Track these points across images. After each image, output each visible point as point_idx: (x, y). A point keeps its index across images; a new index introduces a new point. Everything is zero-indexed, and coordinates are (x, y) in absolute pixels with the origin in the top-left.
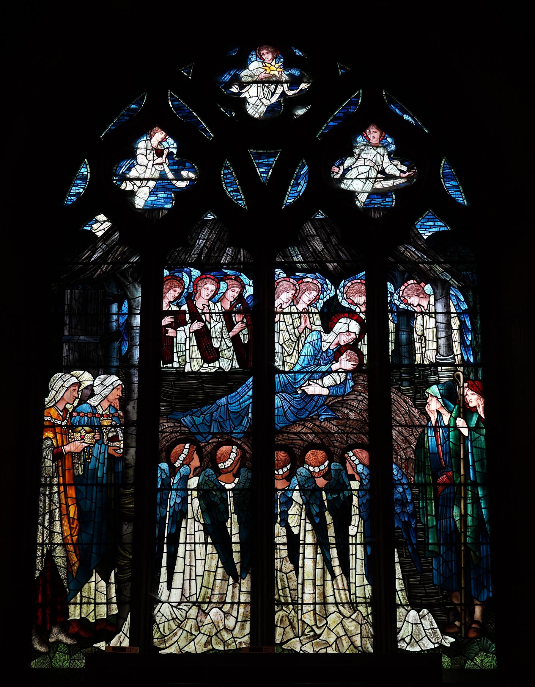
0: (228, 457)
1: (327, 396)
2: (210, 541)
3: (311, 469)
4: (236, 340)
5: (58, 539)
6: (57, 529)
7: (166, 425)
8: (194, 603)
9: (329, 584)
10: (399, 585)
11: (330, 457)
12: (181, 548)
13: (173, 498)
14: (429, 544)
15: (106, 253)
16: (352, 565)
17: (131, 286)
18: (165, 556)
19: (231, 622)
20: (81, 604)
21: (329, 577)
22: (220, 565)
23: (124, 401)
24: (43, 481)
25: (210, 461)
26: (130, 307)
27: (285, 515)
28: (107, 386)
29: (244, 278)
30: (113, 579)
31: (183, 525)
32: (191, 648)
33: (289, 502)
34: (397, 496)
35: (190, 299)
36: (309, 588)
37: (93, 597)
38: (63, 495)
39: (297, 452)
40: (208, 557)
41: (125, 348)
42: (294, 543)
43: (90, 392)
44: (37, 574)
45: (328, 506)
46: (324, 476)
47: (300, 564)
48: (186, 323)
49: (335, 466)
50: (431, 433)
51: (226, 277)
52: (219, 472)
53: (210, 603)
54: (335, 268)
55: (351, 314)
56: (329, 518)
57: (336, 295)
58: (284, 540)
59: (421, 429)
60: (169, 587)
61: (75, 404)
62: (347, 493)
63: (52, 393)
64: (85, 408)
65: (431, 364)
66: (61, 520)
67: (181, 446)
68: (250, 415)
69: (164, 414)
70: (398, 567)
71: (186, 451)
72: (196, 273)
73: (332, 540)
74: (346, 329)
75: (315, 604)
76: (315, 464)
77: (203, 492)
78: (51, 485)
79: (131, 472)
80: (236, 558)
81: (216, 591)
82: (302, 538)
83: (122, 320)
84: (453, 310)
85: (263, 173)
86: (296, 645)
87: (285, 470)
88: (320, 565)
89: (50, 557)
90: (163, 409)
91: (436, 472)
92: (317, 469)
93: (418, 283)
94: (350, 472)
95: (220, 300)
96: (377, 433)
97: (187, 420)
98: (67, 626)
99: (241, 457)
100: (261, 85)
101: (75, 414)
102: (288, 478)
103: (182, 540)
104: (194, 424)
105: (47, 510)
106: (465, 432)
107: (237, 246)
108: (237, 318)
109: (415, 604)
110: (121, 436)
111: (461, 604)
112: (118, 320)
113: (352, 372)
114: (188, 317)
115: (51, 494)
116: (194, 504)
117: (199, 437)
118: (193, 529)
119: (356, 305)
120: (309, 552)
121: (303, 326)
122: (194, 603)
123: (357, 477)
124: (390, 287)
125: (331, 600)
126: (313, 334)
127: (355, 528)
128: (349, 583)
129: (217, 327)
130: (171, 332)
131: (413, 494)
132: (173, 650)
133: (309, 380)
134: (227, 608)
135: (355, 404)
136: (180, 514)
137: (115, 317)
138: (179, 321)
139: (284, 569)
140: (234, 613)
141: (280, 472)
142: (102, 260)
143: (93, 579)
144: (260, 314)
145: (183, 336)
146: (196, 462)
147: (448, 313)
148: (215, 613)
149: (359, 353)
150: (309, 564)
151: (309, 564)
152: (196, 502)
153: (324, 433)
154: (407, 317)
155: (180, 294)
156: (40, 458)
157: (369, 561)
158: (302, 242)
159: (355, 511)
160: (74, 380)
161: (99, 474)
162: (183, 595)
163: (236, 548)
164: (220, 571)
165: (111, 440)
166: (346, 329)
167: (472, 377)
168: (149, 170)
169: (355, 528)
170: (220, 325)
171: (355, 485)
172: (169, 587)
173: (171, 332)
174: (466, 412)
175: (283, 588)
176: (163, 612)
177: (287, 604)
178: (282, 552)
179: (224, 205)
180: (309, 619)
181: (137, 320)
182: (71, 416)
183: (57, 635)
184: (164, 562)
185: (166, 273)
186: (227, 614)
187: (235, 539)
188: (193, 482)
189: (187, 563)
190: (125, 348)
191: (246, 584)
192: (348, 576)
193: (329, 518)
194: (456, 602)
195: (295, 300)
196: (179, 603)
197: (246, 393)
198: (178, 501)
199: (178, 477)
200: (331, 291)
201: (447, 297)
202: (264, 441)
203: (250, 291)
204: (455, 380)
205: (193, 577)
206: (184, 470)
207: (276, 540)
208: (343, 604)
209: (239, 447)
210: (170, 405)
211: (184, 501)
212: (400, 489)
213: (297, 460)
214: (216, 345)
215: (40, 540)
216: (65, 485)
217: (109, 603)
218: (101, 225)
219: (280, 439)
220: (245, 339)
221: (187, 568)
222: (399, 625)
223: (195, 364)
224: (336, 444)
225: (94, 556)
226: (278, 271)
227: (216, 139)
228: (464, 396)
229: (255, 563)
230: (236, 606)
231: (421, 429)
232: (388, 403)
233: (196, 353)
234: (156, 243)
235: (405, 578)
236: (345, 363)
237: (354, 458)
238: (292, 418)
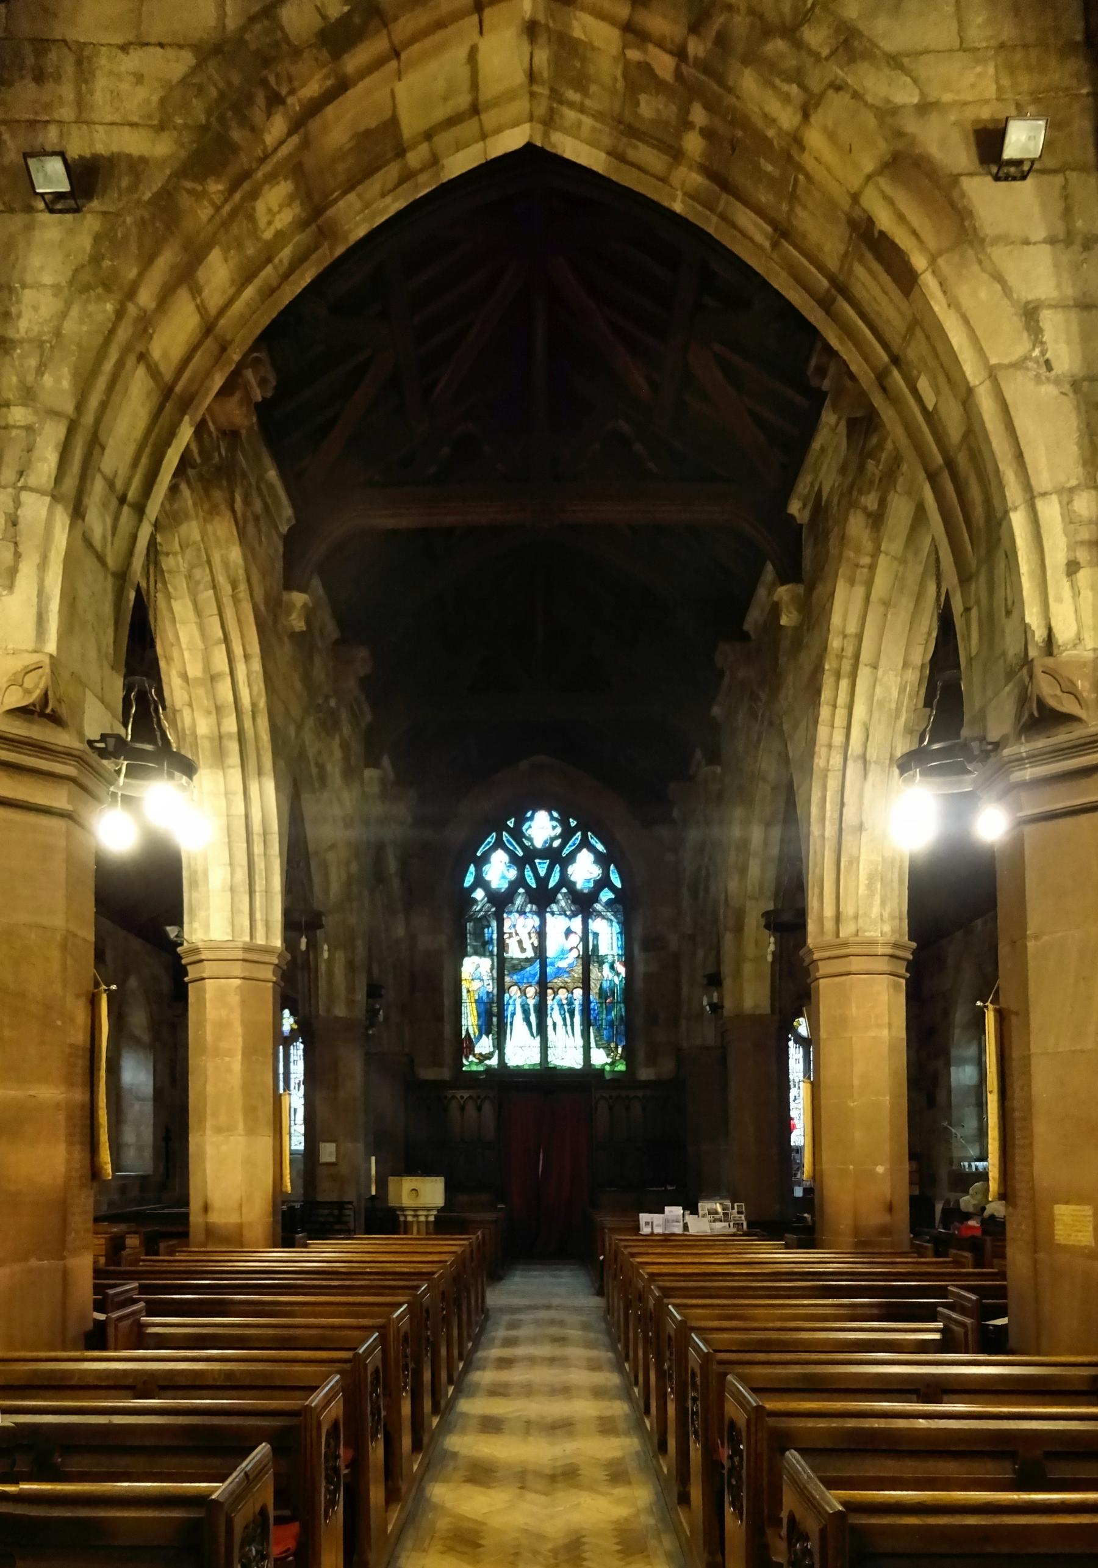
0: (531, 991)
6: (470, 1020)
7: (507, 979)
13: (511, 1008)
25: (524, 993)
35: (514, 926)
43: (478, 966)
72: (517, 915)
74: (575, 940)
77: (523, 1006)
85: (542, 872)
97: (515, 977)
98: (474, 1055)
126: (562, 934)
130: (507, 941)
136: (513, 1014)
142: (481, 910)
144: (541, 933)
146: (519, 994)
181: (495, 936)
183: (471, 1058)
191: (538, 1038)
197: (537, 965)
220: (536, 944)
225: (485, 1028)
233: (518, 949)
234: (501, 902)
236: (575, 953)
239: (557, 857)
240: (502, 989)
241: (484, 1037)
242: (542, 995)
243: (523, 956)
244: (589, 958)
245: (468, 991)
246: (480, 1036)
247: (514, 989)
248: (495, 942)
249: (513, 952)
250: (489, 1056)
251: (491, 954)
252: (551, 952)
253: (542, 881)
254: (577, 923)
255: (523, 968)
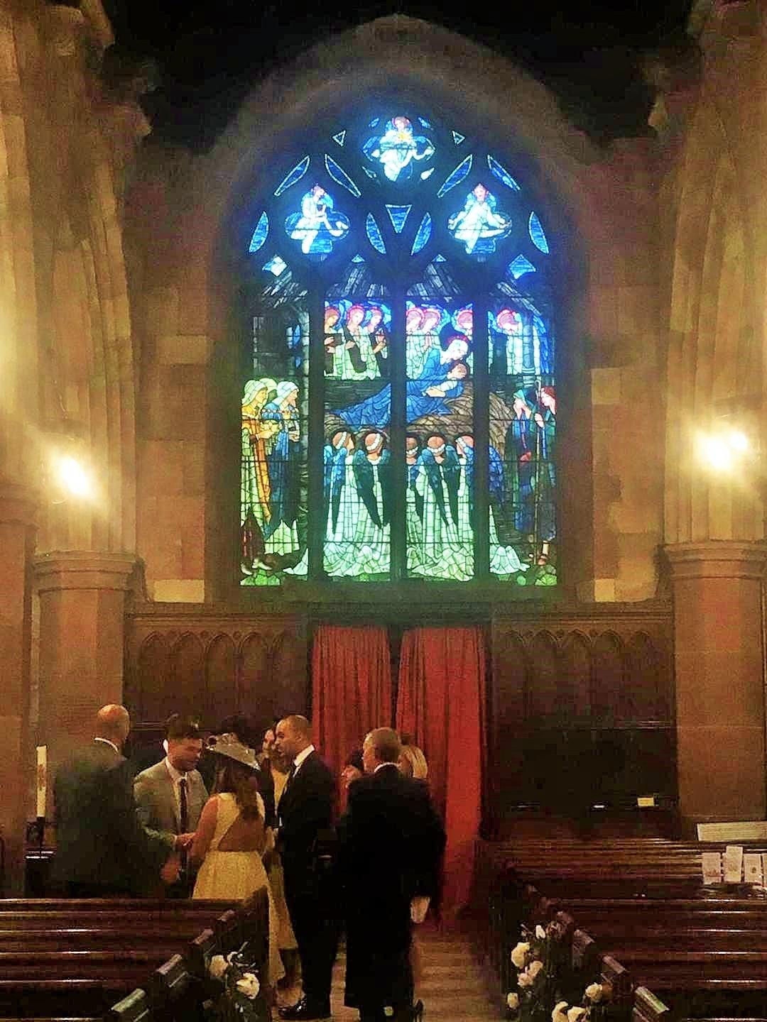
0: (374, 441)
1: (444, 398)
2: (362, 500)
3: (432, 450)
4: (378, 355)
5: (255, 499)
7: (329, 419)
8: (351, 543)
9: (444, 529)
10: (492, 530)
11: (446, 442)
12: (342, 506)
13: (335, 472)
14: (513, 503)
15: (282, 289)
16: (460, 517)
17: (301, 314)
18: (330, 511)
19: (376, 556)
20: (274, 543)
21: (444, 525)
22: (369, 517)
23: (299, 401)
24: (243, 459)
25: (361, 445)
26: (301, 330)
27: (414, 482)
28: (287, 390)
29: (384, 308)
30: (295, 526)
31: (343, 489)
32: (349, 572)
33: (417, 473)
34: (492, 469)
35: (344, 323)
36: (430, 532)
37: (281, 538)
38: (258, 468)
39: (422, 438)
40: (361, 512)
41: (298, 363)
42: (420, 501)
44: (242, 523)
45: (445, 475)
46: (441, 456)
47: (424, 516)
48: (342, 343)
49: (449, 448)
50: (516, 424)
51: (370, 307)
52: (367, 452)
53: (362, 543)
54: (450, 300)
55: (461, 336)
56: (444, 485)
57: (451, 322)
58: (414, 500)
59: (509, 422)
60: (334, 532)
61: (264, 403)
62: (457, 468)
63: (247, 396)
64: (270, 405)
65: (518, 375)
66: (257, 486)
67: (340, 434)
68: (389, 412)
69: (328, 410)
70: (491, 518)
71: (344, 438)
72: (349, 304)
73: (446, 500)
74: (458, 349)
75: (434, 543)
76: (435, 447)
77: (357, 467)
78: (249, 462)
79: (306, 453)
80: (380, 512)
81: (366, 535)
82: (425, 498)
83: (296, 340)
84: (535, 333)
86: (420, 570)
87: (414, 451)
88: (438, 516)
89: (250, 512)
90: (327, 407)
91: (522, 451)
92: (436, 451)
93: (511, 313)
94: (459, 452)
95: (367, 325)
96: (479, 427)
97: (344, 415)
99: (383, 442)
100: (397, 149)
101: (264, 411)
102: (416, 457)
103: (342, 500)
104: (349, 418)
105: (247, 479)
106: (541, 424)
107: (379, 283)
108: (379, 339)
109: (503, 543)
110: (298, 427)
111: (533, 543)
112: (293, 341)
113: (463, 380)
114: (343, 338)
115: (250, 468)
116: (350, 476)
117: (353, 428)
118: (350, 492)
119: (466, 329)
120: (430, 508)
121: (427, 345)
122: (351, 543)
123: (464, 456)
124: (490, 315)
125: (445, 540)
126: (433, 342)
127: (463, 491)
128: (458, 529)
129: (364, 345)
131: (503, 468)
132: (338, 573)
133: (431, 385)
134: (374, 546)
135: (463, 403)
136: (341, 482)
137: (290, 339)
138: (336, 344)
139: (413, 520)
140: (379, 549)
141: (411, 452)
143: (281, 526)
144: (395, 336)
145: (340, 354)
146: (351, 445)
147: (531, 336)
148: (366, 550)
149: (468, 367)
150: (430, 517)
151: (430, 517)
152: (352, 474)
153: (441, 425)
154: (502, 339)
155: (338, 320)
156: (240, 443)
157: (472, 515)
158: (426, 280)
159: (462, 480)
160: (263, 386)
161: (283, 454)
162: (343, 537)
163: (380, 506)
164: (369, 521)
165: (289, 429)
166: (458, 349)
167: (547, 384)
168: (313, 221)
169: (463, 491)
170: (367, 344)
171: (463, 461)
172: (334, 532)
173: (331, 350)
174: (543, 409)
175: (413, 533)
176: (329, 549)
177: (415, 543)
178: (412, 508)
179: (367, 251)
180: (430, 553)
181: (306, 341)
182: (261, 413)
183: (257, 564)
184: (330, 515)
185: (327, 304)
186: (374, 550)
187: (379, 499)
188: (349, 460)
189: (346, 515)
190: (298, 363)
191: (387, 529)
192: (457, 525)
193: (444, 485)
194: (531, 541)
195: (421, 325)
196: (341, 543)
198: (339, 472)
199: (338, 456)
200: (447, 319)
201: (531, 323)
202: (399, 430)
203: (388, 318)
204: (535, 387)
205: (350, 525)
206: (341, 452)
207: (408, 500)
208: (453, 543)
209: (382, 435)
210: (332, 404)
211: (343, 473)
212: (494, 464)
213: (422, 444)
214: (364, 359)
215: (243, 500)
216: (259, 462)
217: (293, 543)
218: (277, 266)
219: (411, 429)
220: (385, 356)
221: (346, 519)
222: (491, 556)
223: (349, 373)
224: (450, 432)
225: (286, 510)
226: (408, 303)
227: (363, 197)
228: (540, 398)
229: (393, 515)
230: (380, 544)
231: (509, 422)
232: (488, 403)
233: (350, 365)
234: (319, 280)
235: (497, 527)
236: (457, 373)
237: (462, 443)
238: (419, 414)
239: (429, 199)
240: (319, 438)
241: (283, 525)
242: (394, 448)
243: (359, 377)
244: (489, 378)
245: (253, 441)
246: (274, 526)
247: (342, 438)
248: (306, 350)
249: (342, 368)
250: (292, 560)
251: (298, 377)
252: (415, 368)
253: (399, 243)
254: (464, 322)
255: (359, 400)
